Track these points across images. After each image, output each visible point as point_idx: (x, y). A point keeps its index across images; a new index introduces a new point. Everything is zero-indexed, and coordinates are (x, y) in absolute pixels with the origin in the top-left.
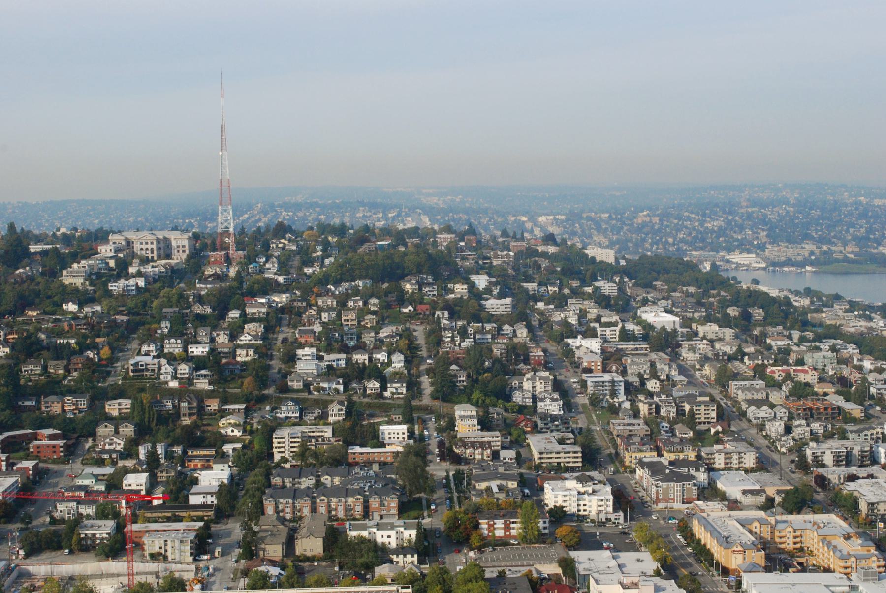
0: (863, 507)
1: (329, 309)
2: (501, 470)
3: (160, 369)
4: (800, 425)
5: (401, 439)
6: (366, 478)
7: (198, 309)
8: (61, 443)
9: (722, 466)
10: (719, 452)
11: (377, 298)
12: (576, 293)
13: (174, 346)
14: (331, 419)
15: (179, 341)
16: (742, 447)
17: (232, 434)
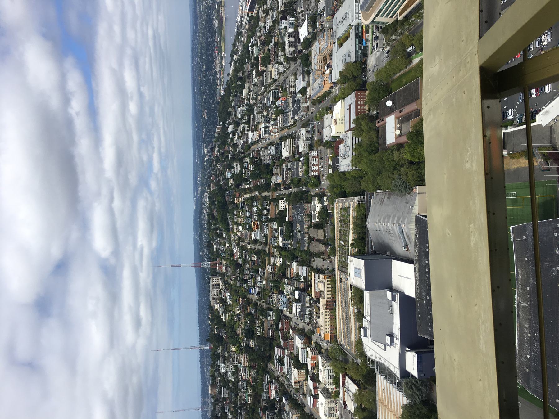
0: (309, 37)
1: (238, 229)
2: (295, 167)
3: (259, 287)
4: (280, 59)
5: (284, 203)
6: (297, 215)
7: (237, 274)
8: (284, 321)
9: (294, 88)
10: (289, 89)
11: (234, 211)
12: (232, 140)
13: (250, 283)
14: (277, 227)
15: (249, 280)
16: (288, 81)
17: (281, 262)
